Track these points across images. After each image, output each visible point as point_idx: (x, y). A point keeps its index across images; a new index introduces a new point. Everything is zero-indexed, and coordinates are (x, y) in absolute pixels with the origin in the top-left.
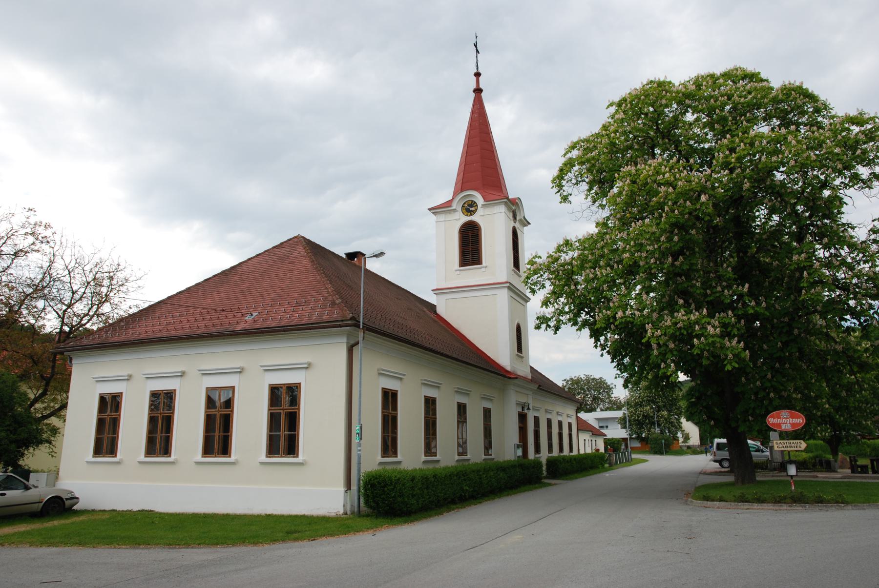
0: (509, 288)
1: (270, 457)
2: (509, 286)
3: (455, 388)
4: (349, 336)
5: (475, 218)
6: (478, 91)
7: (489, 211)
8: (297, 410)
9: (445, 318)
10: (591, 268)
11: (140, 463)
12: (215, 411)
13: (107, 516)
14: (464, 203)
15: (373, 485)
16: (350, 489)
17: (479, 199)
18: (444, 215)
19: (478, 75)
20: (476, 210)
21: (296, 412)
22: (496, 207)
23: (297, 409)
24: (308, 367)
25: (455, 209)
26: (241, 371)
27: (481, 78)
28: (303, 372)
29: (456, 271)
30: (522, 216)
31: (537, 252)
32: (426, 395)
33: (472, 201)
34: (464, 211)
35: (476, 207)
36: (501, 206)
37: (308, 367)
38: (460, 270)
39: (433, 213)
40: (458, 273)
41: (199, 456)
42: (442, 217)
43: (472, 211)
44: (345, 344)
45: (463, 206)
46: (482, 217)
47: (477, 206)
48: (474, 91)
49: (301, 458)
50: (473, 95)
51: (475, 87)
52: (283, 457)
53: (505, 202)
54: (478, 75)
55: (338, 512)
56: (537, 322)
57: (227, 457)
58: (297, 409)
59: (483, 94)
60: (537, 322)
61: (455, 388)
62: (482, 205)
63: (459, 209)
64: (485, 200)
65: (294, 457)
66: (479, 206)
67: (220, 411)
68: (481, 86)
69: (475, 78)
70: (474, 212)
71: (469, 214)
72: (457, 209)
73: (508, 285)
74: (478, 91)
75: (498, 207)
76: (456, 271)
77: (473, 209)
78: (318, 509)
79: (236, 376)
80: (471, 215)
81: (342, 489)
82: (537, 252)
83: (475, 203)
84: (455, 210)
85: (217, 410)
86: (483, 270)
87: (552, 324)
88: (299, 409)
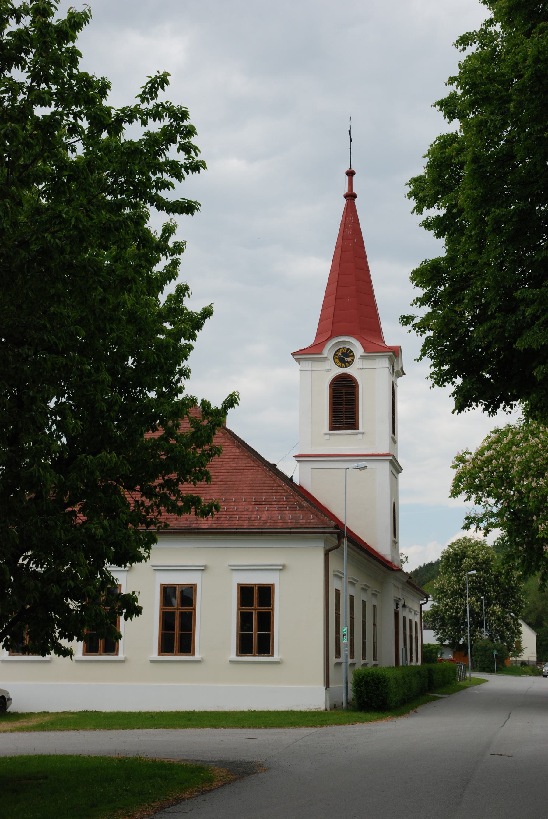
0: (391, 462)
1: (241, 656)
2: (391, 460)
3: (362, 584)
4: (326, 541)
5: (348, 370)
6: (351, 197)
7: (369, 364)
8: (270, 610)
9: (310, 491)
10: (533, 476)
11: (152, 661)
12: (174, 609)
13: (47, 719)
14: (337, 351)
15: (367, 683)
16: (329, 687)
17: (358, 349)
18: (310, 363)
19: (351, 174)
20: (353, 360)
21: (163, 606)
22: (377, 360)
23: (272, 609)
24: (282, 568)
25: (326, 357)
26: (204, 569)
27: (354, 178)
28: (277, 574)
29: (325, 434)
30: (400, 367)
31: (467, 448)
32: (351, 594)
33: (348, 349)
34: (337, 360)
35: (352, 358)
36: (384, 360)
37: (282, 568)
38: (331, 435)
39: (297, 359)
40: (327, 437)
41: (233, 655)
42: (307, 365)
43: (347, 362)
44: (323, 548)
45: (335, 354)
46: (360, 371)
47: (353, 355)
48: (346, 196)
49: (276, 657)
50: (345, 201)
51: (346, 191)
52: (256, 656)
53: (390, 356)
54: (351, 174)
55: (320, 708)
56: (466, 521)
57: (190, 655)
58: (272, 609)
59: (356, 201)
60: (466, 521)
61: (362, 584)
62: (361, 356)
63: (331, 357)
64: (366, 350)
65: (268, 656)
66: (357, 356)
67: (180, 609)
68: (355, 191)
69: (347, 177)
70: (350, 364)
71: (344, 365)
72: (329, 358)
73: (391, 458)
74: (351, 197)
75: (381, 360)
76: (325, 434)
77: (349, 359)
78: (298, 706)
79: (199, 574)
80: (346, 367)
81: (323, 688)
82: (467, 448)
83: (351, 351)
84: (325, 359)
85: (179, 611)
86: (360, 436)
87: (483, 525)
88: (273, 609)
